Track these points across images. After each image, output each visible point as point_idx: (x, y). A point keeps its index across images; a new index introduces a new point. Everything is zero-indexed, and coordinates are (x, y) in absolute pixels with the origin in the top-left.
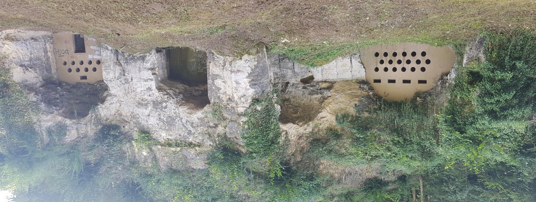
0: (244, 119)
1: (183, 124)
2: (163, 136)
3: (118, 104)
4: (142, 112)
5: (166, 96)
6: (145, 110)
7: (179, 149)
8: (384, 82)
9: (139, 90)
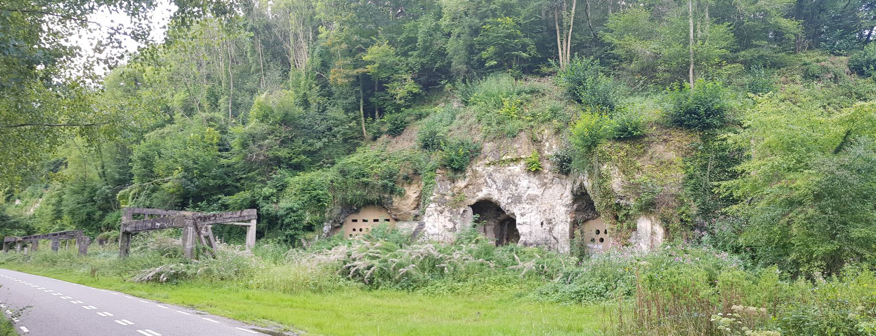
0: (432, 198)
1: (495, 182)
2: (517, 169)
3: (564, 195)
4: (535, 191)
5: (507, 209)
6: (531, 193)
7: (504, 158)
8: (381, 220)
9: (534, 213)
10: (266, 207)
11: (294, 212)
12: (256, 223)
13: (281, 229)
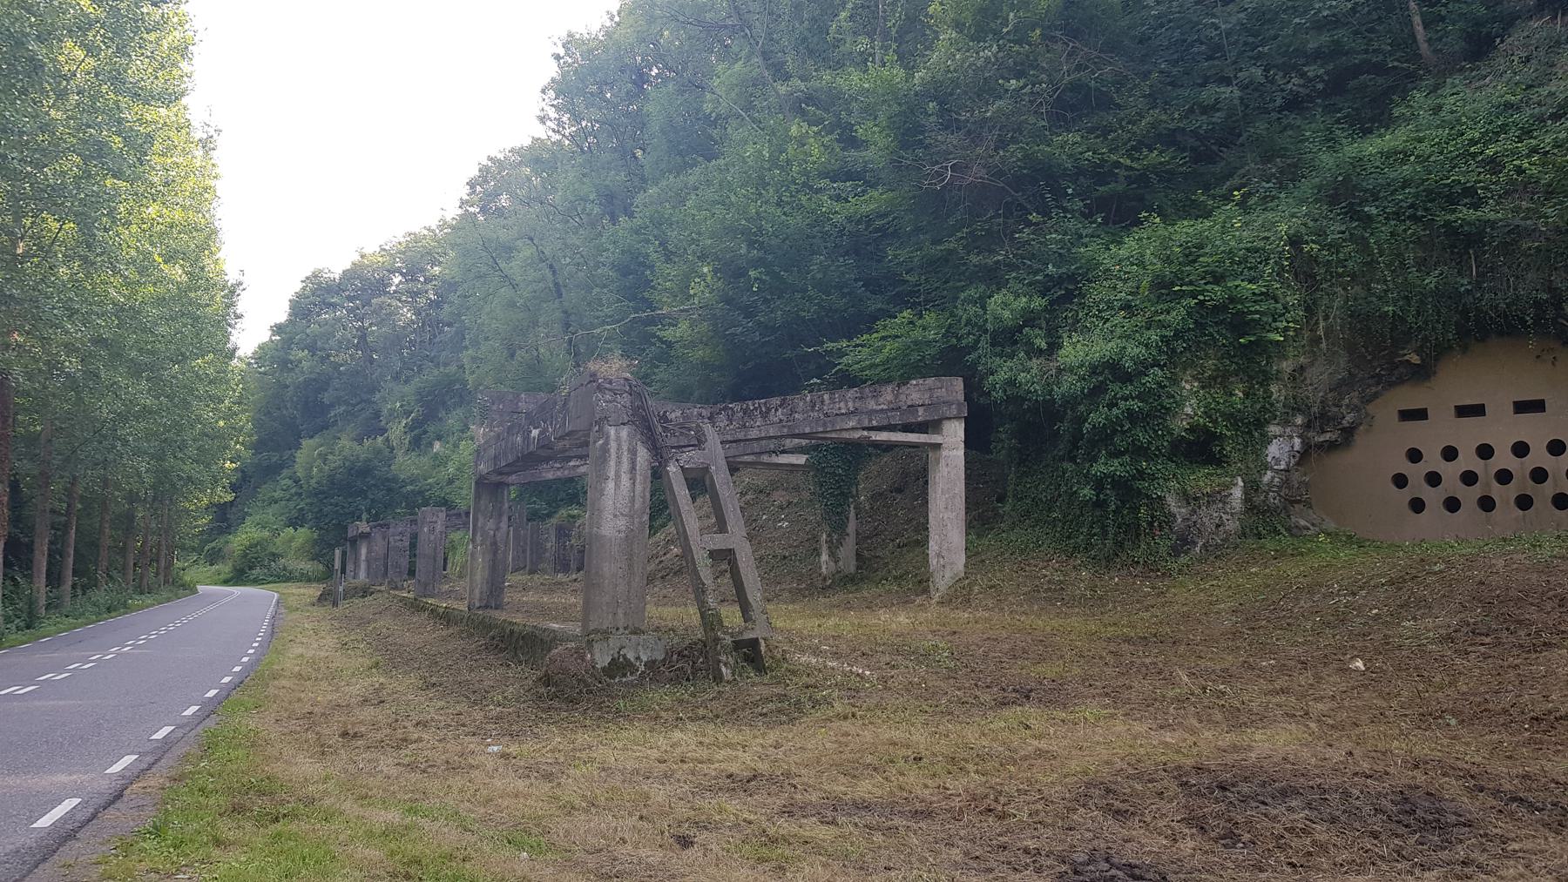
10: (1003, 371)
11: (1126, 378)
12: (961, 434)
13: (1073, 459)
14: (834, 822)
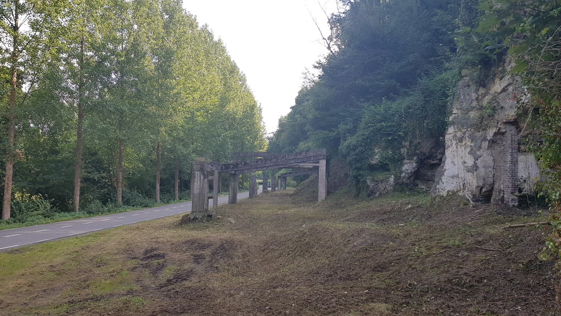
14: (322, 264)
